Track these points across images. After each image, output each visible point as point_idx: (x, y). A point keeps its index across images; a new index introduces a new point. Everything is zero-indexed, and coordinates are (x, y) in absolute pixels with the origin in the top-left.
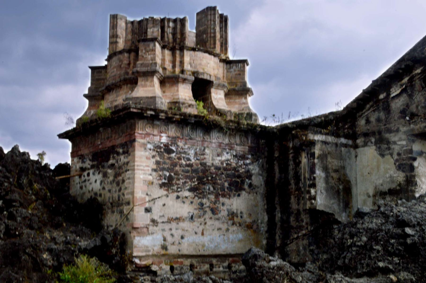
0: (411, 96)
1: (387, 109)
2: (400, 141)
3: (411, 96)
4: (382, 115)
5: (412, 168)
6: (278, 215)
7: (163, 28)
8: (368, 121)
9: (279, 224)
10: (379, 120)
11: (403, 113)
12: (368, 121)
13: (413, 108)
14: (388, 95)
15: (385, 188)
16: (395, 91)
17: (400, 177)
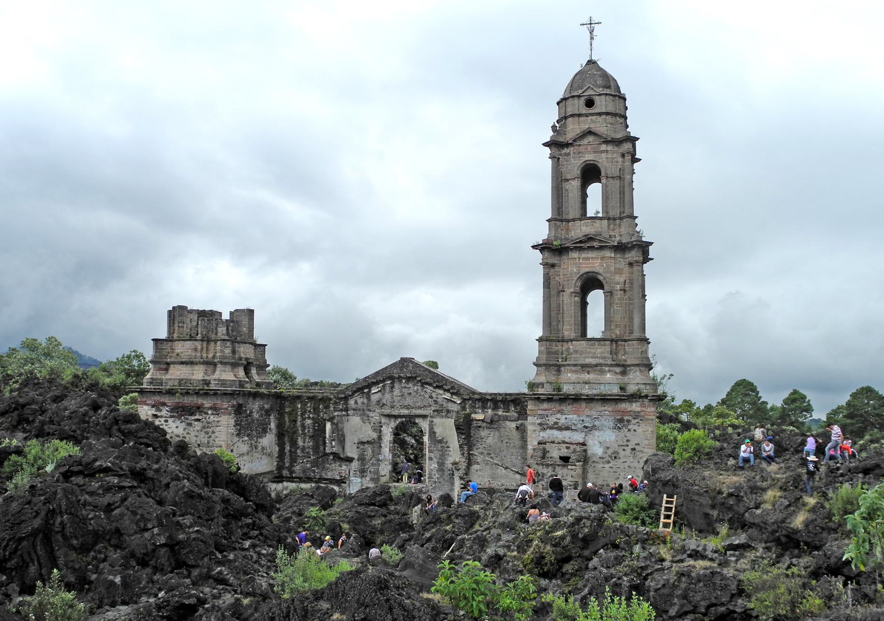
0: (383, 394)
1: (369, 398)
2: (375, 416)
3: (383, 394)
4: (365, 401)
5: (381, 431)
6: (288, 448)
7: (228, 327)
8: (356, 402)
9: (288, 454)
10: (363, 403)
11: (378, 402)
12: (356, 402)
13: (384, 401)
14: (370, 391)
15: (365, 440)
16: (374, 390)
17: (375, 435)
